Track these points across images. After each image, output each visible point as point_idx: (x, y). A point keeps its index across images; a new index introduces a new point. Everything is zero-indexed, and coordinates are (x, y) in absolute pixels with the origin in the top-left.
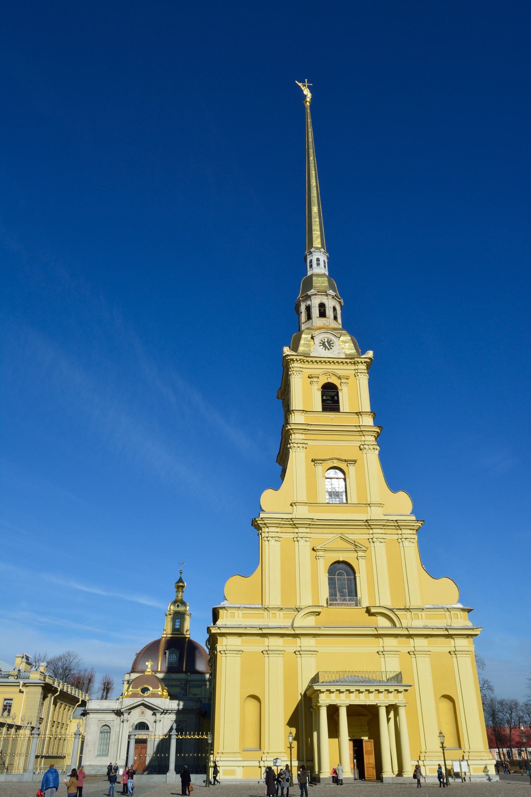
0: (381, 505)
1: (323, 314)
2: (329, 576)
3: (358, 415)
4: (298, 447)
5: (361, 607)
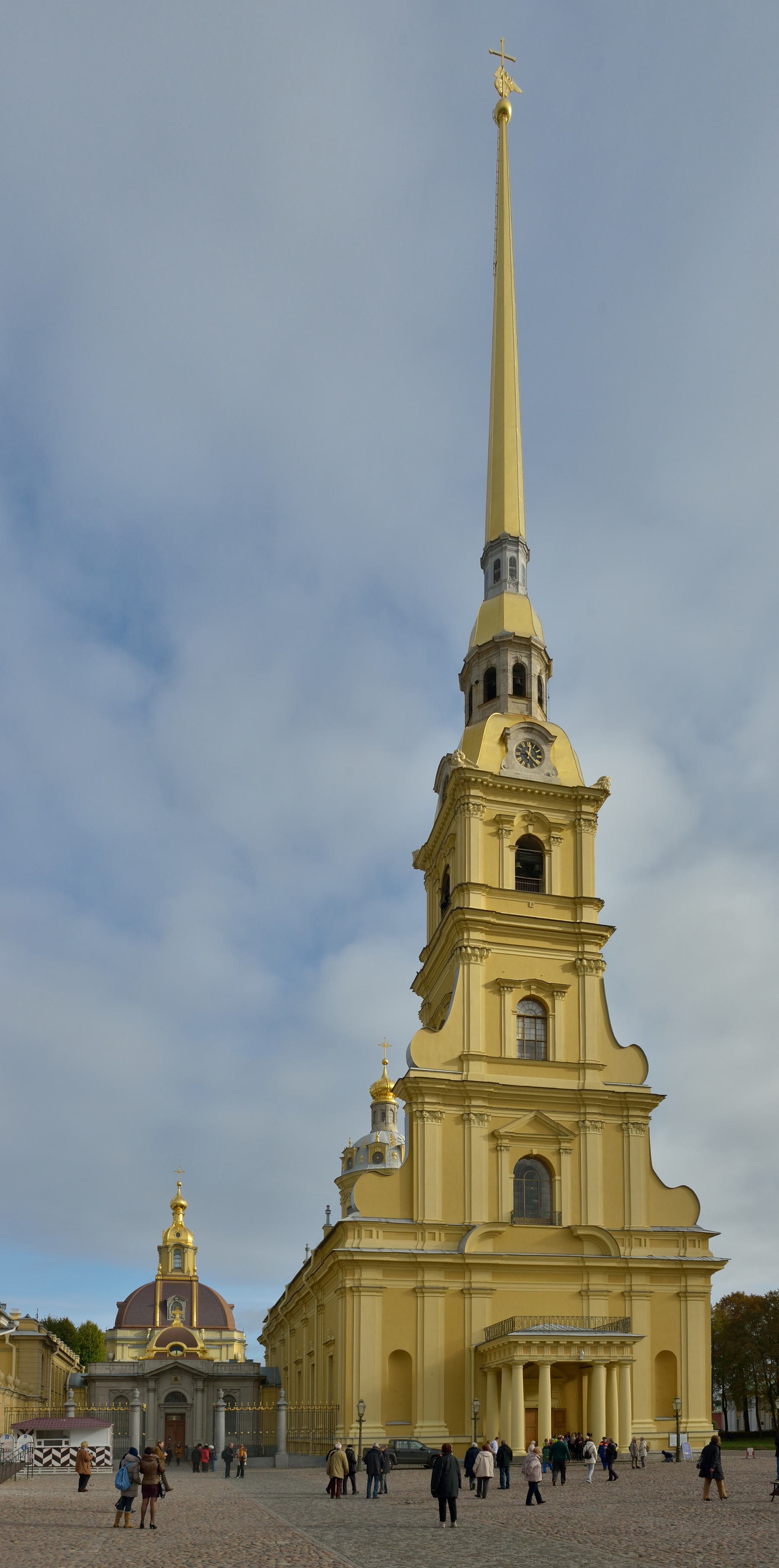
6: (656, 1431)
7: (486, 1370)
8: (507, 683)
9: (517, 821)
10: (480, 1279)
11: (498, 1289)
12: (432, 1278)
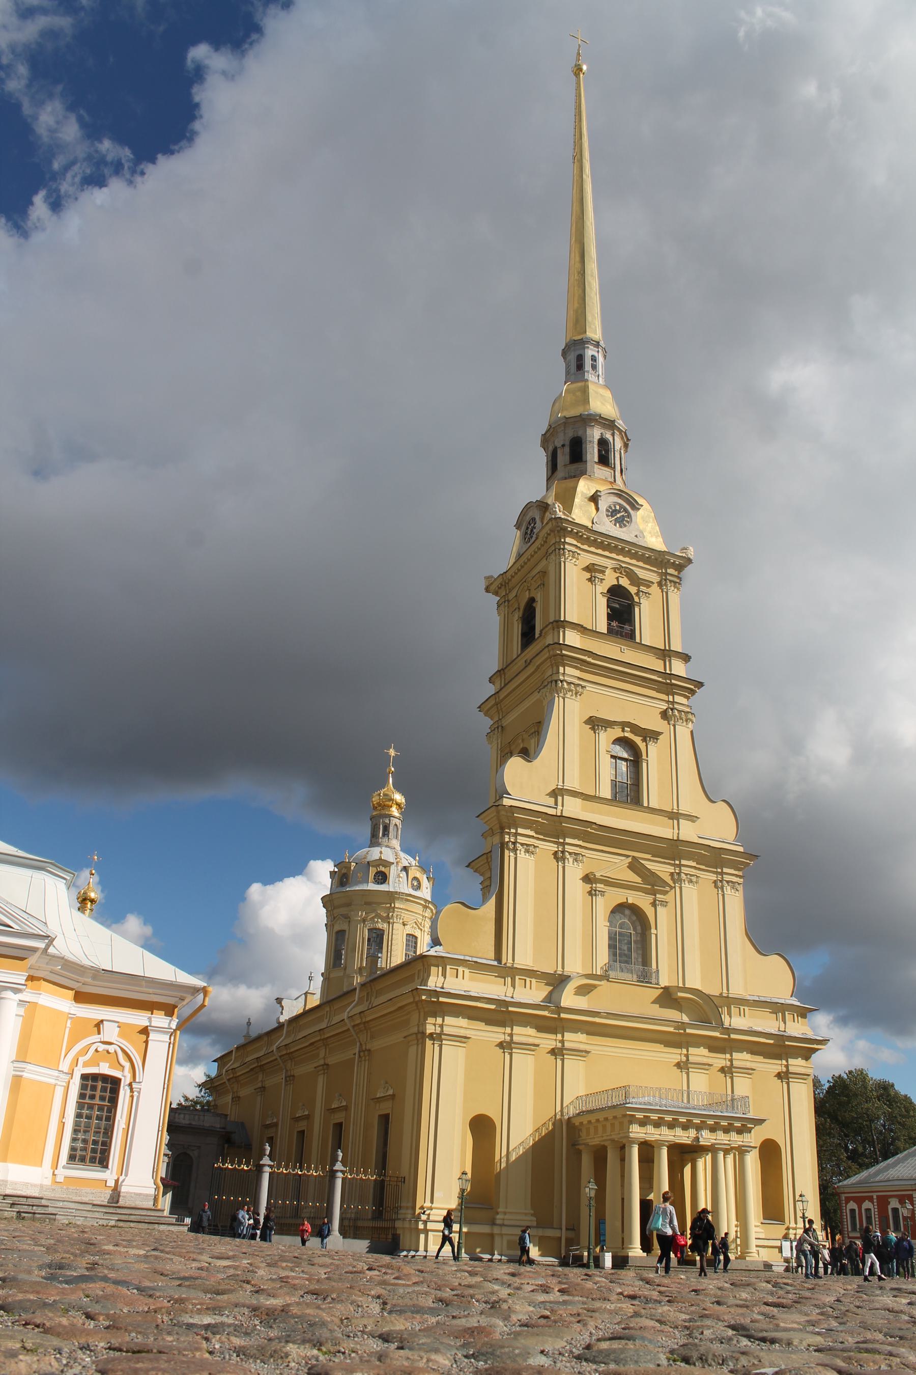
0: (692, 818)
1: (604, 460)
2: (611, 926)
3: (664, 656)
4: (570, 690)
5: (659, 987)
6: (764, 1237)
7: (581, 1147)
8: (592, 453)
9: (608, 572)
10: (573, 1039)
11: (593, 1052)
12: (524, 1033)
